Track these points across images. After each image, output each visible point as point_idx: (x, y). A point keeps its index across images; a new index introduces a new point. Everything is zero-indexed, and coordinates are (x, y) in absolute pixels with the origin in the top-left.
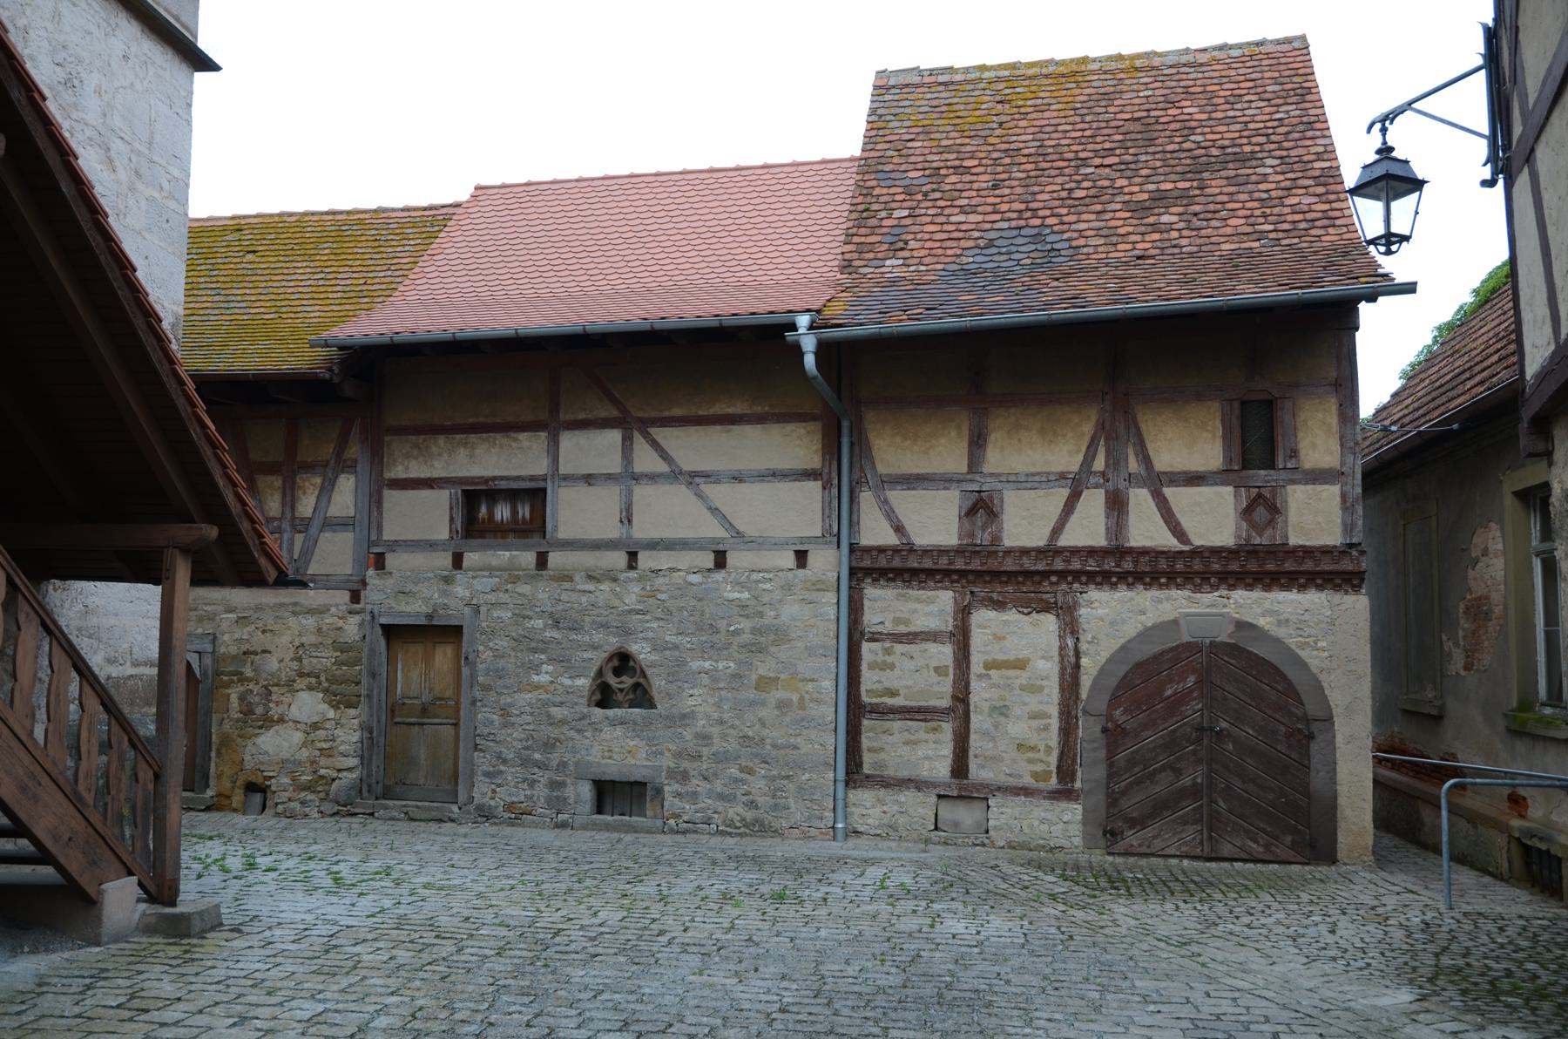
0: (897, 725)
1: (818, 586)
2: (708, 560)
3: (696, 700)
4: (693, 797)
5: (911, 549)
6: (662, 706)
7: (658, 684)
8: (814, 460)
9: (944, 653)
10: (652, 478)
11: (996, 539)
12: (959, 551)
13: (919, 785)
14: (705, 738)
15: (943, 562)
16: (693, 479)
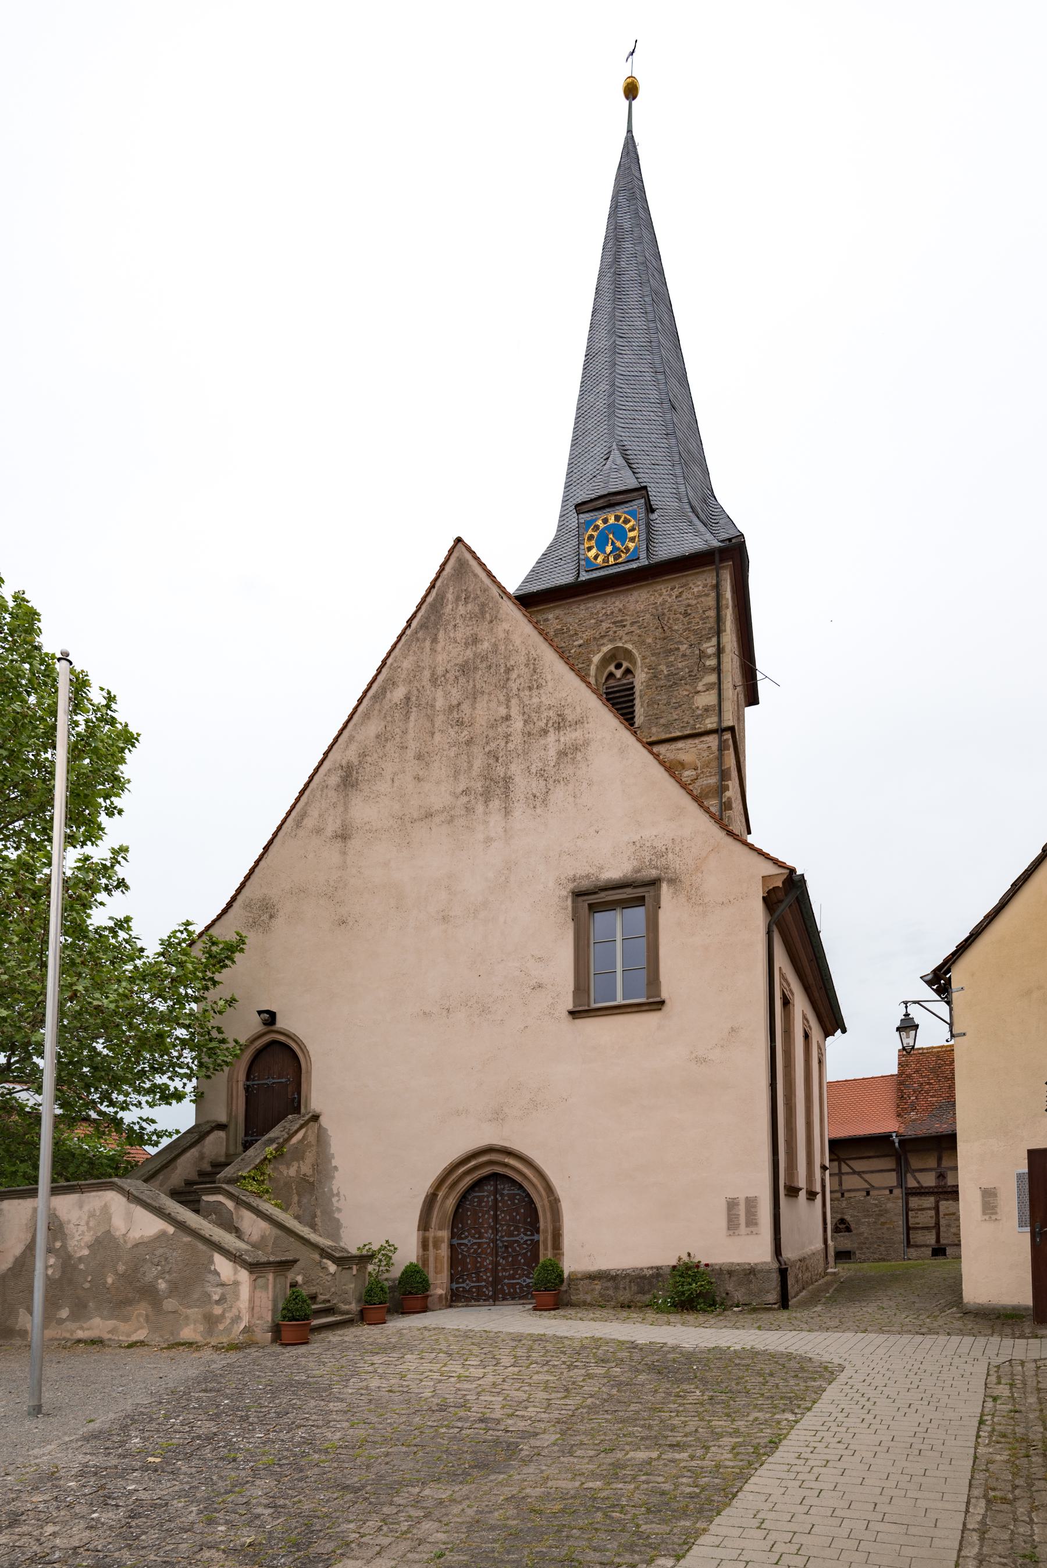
0: (920, 1232)
1: (897, 1198)
2: (865, 1193)
3: (863, 1229)
4: (864, 1254)
5: (922, 1187)
6: (854, 1232)
7: (853, 1226)
8: (894, 1166)
9: (933, 1213)
10: (847, 1173)
11: (946, 1184)
12: (936, 1187)
13: (927, 1246)
14: (867, 1238)
15: (931, 1190)
16: (859, 1173)
